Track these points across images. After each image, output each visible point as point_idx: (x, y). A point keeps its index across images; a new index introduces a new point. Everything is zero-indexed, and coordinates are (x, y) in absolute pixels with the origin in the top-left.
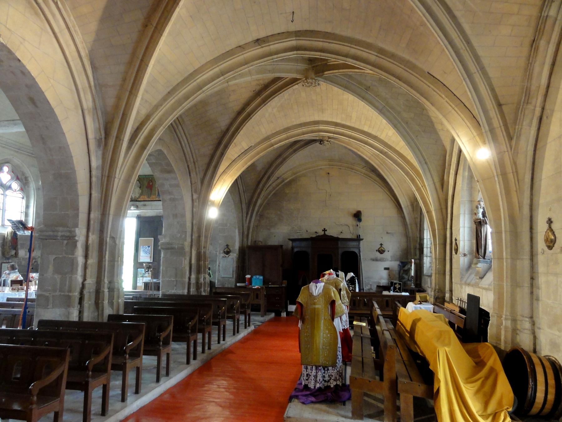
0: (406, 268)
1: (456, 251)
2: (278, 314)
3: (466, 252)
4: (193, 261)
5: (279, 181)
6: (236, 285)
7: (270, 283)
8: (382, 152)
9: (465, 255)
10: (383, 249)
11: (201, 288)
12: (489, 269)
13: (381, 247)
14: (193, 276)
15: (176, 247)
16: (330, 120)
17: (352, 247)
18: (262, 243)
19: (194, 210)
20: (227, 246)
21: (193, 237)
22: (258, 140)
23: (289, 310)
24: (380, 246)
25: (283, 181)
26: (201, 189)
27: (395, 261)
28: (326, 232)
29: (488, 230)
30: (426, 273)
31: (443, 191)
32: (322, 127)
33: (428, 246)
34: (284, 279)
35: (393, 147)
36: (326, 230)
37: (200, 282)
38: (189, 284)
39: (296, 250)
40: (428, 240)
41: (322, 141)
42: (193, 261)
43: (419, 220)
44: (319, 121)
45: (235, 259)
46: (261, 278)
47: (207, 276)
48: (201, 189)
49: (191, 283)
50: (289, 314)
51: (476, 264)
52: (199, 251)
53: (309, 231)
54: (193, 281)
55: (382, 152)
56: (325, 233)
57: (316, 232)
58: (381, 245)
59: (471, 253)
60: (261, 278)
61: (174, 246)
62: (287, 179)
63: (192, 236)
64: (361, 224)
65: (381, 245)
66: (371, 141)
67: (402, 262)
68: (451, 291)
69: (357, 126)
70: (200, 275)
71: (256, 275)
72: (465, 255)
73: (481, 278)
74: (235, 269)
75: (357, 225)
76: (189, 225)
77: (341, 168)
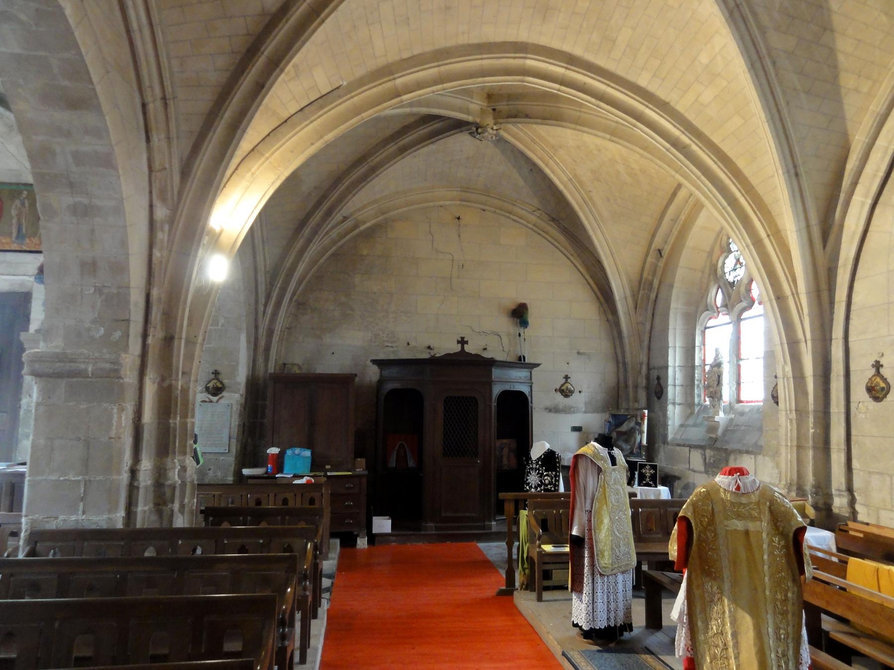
0: (624, 428)
2: (348, 541)
4: (148, 416)
5: (348, 224)
6: (238, 474)
7: (328, 467)
8: (675, 144)
10: (570, 386)
11: (173, 502)
13: (566, 382)
14: (146, 465)
15: (90, 369)
16: (556, 45)
17: (516, 380)
18: (300, 368)
19: (157, 254)
20: (216, 373)
21: (150, 340)
22: (360, 72)
23: (375, 530)
24: (564, 380)
25: (356, 226)
26: (180, 194)
27: (598, 412)
28: (465, 345)
30: (674, 439)
31: (824, 247)
32: (532, 63)
33: (677, 382)
34: (358, 454)
35: (706, 136)
36: (467, 342)
37: (169, 482)
38: (132, 489)
39: (390, 386)
40: (677, 368)
41: (481, 127)
42: (148, 416)
43: (648, 327)
44: (527, 44)
45: (236, 408)
46: (308, 453)
47: (189, 461)
48: (180, 194)
49: (138, 488)
50: (373, 539)
52: (166, 384)
53: (413, 344)
54: (145, 479)
55: (675, 144)
56: (463, 347)
57: (429, 348)
58: (567, 377)
60: (308, 453)
61: (82, 366)
62: (364, 223)
63: (145, 336)
64: (527, 332)
65: (567, 377)
66: (651, 114)
67: (614, 416)
69: (621, 72)
70: (169, 459)
71: (291, 446)
74: (235, 431)
75: (520, 335)
76: (137, 298)
77: (486, 208)
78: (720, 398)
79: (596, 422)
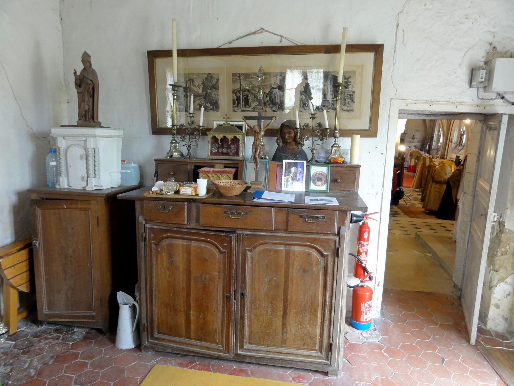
0: (424, 146)
1: (451, 142)
3: (455, 143)
9: (454, 144)
12: (462, 149)
27: (419, 143)
29: (465, 137)
51: (458, 147)
58: (414, 135)
59: (457, 143)
65: (414, 135)
68: (447, 155)
72: (454, 144)
73: (460, 151)
78: (440, 141)
79: (419, 144)
